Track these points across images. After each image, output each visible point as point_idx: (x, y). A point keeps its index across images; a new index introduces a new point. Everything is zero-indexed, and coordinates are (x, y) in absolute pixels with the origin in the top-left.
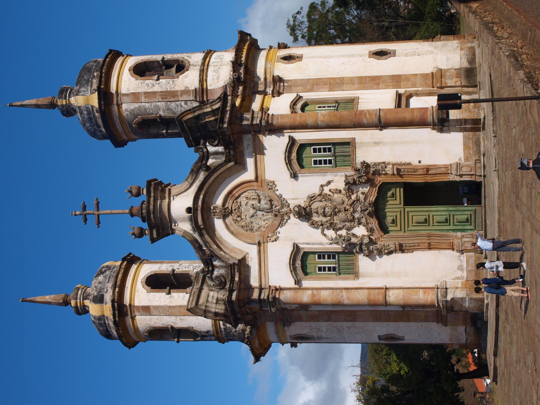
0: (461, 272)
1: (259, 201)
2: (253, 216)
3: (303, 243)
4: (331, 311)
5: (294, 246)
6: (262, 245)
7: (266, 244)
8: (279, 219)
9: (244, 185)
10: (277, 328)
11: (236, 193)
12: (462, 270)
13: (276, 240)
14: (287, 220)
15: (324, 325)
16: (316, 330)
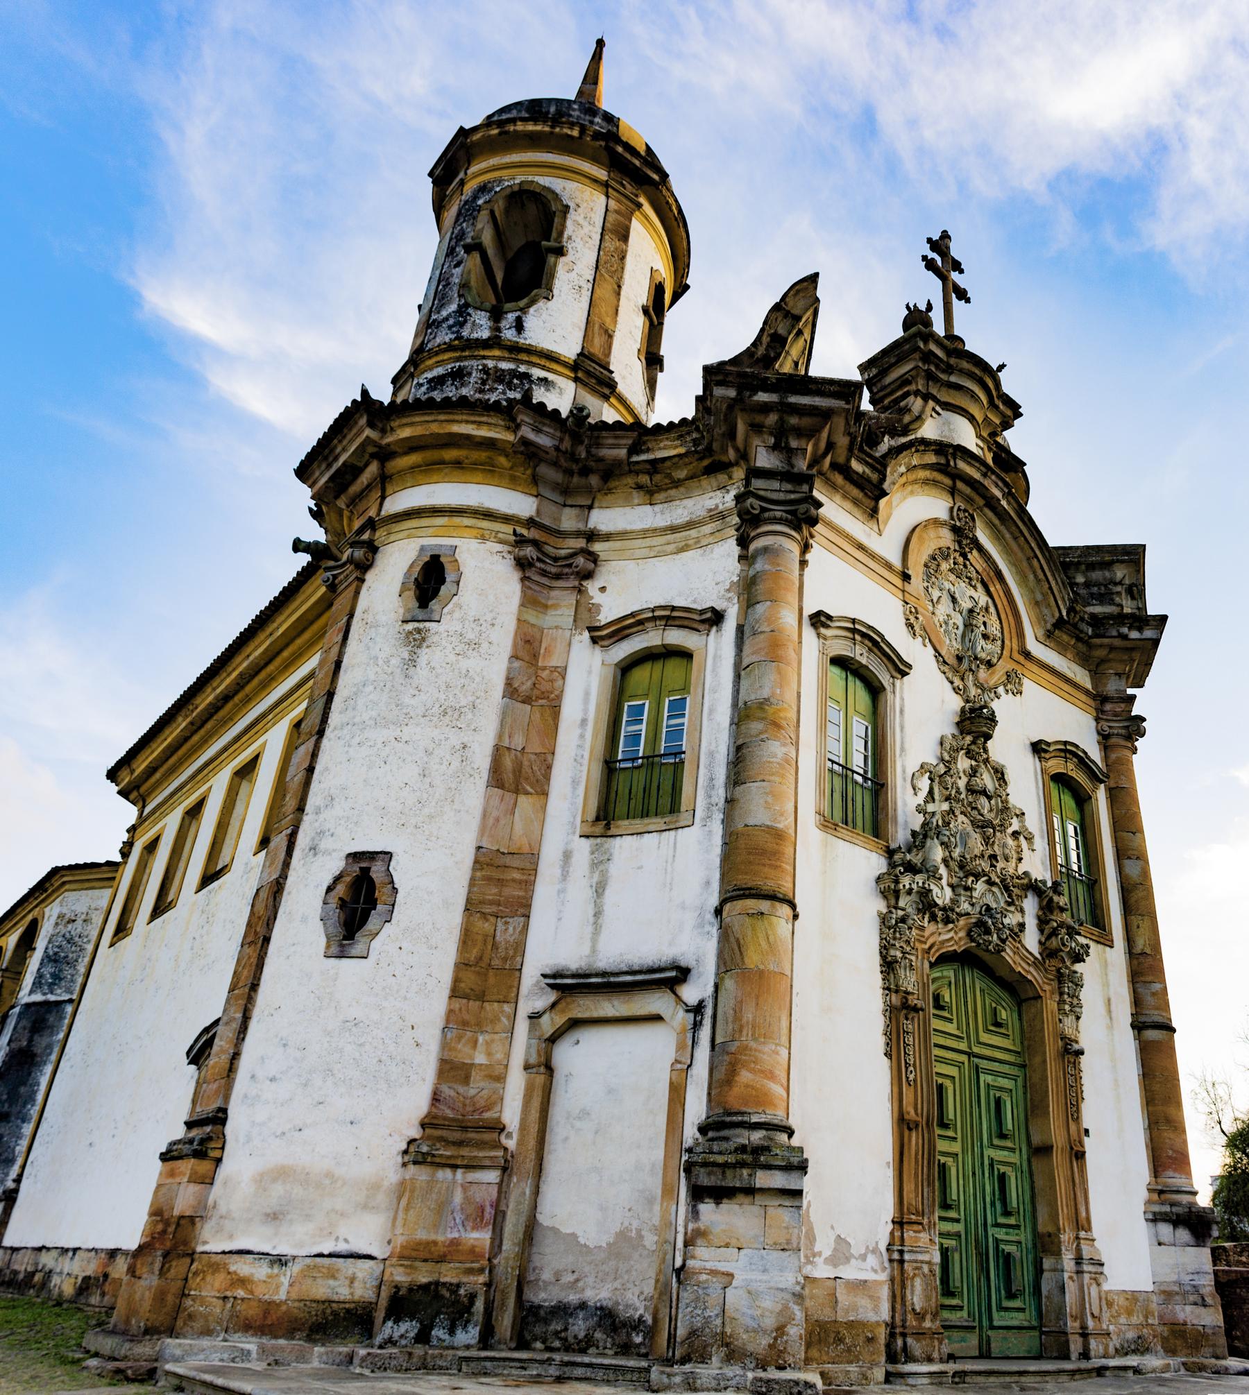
0: (827, 1253)
1: (985, 637)
2: (954, 600)
3: (902, 699)
4: (555, 710)
5: (910, 667)
6: (898, 582)
7: (900, 594)
8: (952, 661)
9: (1011, 618)
10: (506, 519)
11: (995, 588)
12: (833, 1261)
13: (910, 626)
14: (952, 683)
15: (493, 666)
16: (470, 636)
